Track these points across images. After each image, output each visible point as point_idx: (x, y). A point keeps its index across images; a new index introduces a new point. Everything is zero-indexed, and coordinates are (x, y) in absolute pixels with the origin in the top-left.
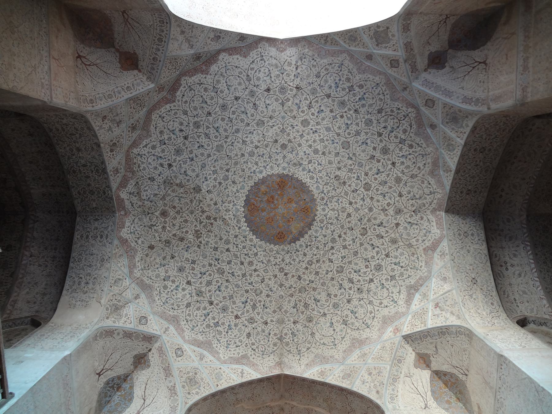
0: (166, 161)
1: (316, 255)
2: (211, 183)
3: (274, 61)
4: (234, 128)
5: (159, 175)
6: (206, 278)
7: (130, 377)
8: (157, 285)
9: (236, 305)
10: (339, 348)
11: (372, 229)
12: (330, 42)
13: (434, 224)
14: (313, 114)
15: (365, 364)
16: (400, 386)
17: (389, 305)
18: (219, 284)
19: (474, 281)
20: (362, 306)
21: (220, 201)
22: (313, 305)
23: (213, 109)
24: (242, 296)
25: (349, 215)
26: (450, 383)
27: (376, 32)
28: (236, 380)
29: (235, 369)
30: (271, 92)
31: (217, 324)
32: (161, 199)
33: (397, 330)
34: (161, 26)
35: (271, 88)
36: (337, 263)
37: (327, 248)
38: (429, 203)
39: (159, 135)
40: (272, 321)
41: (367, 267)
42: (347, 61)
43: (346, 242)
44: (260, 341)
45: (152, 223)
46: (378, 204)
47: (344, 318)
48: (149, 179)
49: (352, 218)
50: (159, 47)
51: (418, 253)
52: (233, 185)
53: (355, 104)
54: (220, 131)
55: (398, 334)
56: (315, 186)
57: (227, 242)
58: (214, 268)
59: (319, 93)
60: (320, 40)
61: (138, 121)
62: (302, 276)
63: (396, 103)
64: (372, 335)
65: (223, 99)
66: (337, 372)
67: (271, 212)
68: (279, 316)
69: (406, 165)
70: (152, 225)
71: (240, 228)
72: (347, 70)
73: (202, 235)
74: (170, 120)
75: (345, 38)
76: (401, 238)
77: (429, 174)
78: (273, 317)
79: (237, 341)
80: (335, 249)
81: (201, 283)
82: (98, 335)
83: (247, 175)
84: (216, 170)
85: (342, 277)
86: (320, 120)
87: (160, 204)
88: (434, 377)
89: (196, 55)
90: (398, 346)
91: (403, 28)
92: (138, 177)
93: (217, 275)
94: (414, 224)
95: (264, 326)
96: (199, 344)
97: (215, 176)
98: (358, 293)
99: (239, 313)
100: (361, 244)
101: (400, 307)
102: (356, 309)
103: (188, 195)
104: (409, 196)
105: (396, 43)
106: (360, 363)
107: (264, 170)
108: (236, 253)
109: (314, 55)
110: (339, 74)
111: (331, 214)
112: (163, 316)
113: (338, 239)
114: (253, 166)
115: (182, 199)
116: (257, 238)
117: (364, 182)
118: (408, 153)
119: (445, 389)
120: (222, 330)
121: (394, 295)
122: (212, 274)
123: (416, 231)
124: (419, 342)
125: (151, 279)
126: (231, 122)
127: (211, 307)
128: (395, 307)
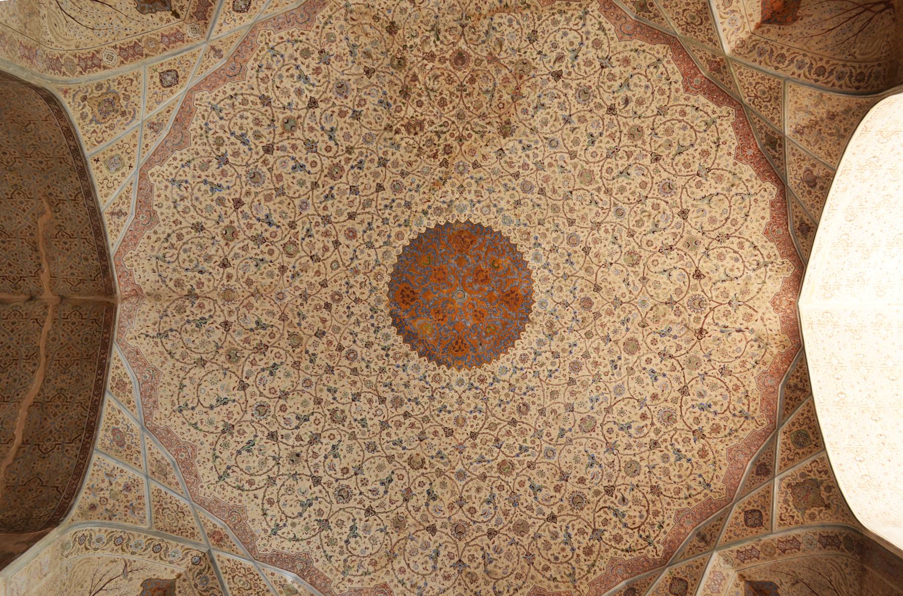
0: (567, 67)
1: (367, 367)
2: (519, 157)
3: (754, 288)
4: (626, 208)
5: (540, 53)
6: (322, 141)
8: (312, 35)
9: (263, 202)
10: (175, 419)
11: (422, 479)
12: (794, 395)
14: (649, 361)
15: (147, 477)
17: (268, 518)
18: (308, 167)
20: (263, 463)
21: (482, 174)
22: (263, 362)
23: (666, 167)
24: (283, 215)
25: (449, 433)
27: (817, 484)
28: (106, 202)
29: (127, 198)
30: (694, 281)
31: (223, 160)
32: (490, 54)
33: (219, 538)
34: (851, 76)
35: (703, 281)
36: (353, 411)
37: (381, 389)
39: (620, 57)
40: (229, 277)
41: (345, 470)
42: (753, 426)
43: (394, 428)
44: (185, 251)
45: (443, 33)
46: (474, 489)
47: (237, 428)
48: (535, 32)
49: (444, 439)
50: (806, 69)
51: (378, 573)
52: (512, 201)
53: (668, 444)
54: (620, 179)
56: (508, 365)
57: (397, 187)
58: (342, 158)
59: (690, 374)
60: (797, 377)
61: (656, 16)
62: (324, 340)
63: (672, 522)
64: (205, 486)
65: (684, 187)
67: (456, 277)
68: (239, 291)
69: (552, 542)
70: (439, 31)
71: (425, 213)
72: (735, 428)
73: (412, 136)
74: (649, 80)
75: (801, 425)
76: (405, 538)
77: (535, 587)
78: (237, 280)
79: (187, 203)
80: (380, 406)
81: (311, 129)
83: (532, 230)
84: (543, 169)
85: (322, 420)
86: (637, 374)
87: (482, 51)
89: (780, 138)
91: (828, 536)
92: (540, 8)
93: (327, 163)
94: (436, 562)
95: (219, 261)
97: (532, 166)
98: (291, 455)
99: (245, 208)
100: (390, 458)
101: (265, 542)
102: (256, 452)
103: (497, 110)
104: (491, 552)
105: (797, 522)
106: (148, 464)
107: (540, 264)
108: (374, 204)
109: (765, 364)
110: (727, 412)
112: (247, 43)
113: (401, 411)
114: (548, 243)
115: (488, 97)
116: (404, 247)
117: (516, 462)
118: (576, 545)
120: (209, 172)
121: (289, 528)
122: (331, 154)
123: (420, 569)
125: (326, 24)
126: (639, 202)
127: (260, 148)
128: (265, 531)
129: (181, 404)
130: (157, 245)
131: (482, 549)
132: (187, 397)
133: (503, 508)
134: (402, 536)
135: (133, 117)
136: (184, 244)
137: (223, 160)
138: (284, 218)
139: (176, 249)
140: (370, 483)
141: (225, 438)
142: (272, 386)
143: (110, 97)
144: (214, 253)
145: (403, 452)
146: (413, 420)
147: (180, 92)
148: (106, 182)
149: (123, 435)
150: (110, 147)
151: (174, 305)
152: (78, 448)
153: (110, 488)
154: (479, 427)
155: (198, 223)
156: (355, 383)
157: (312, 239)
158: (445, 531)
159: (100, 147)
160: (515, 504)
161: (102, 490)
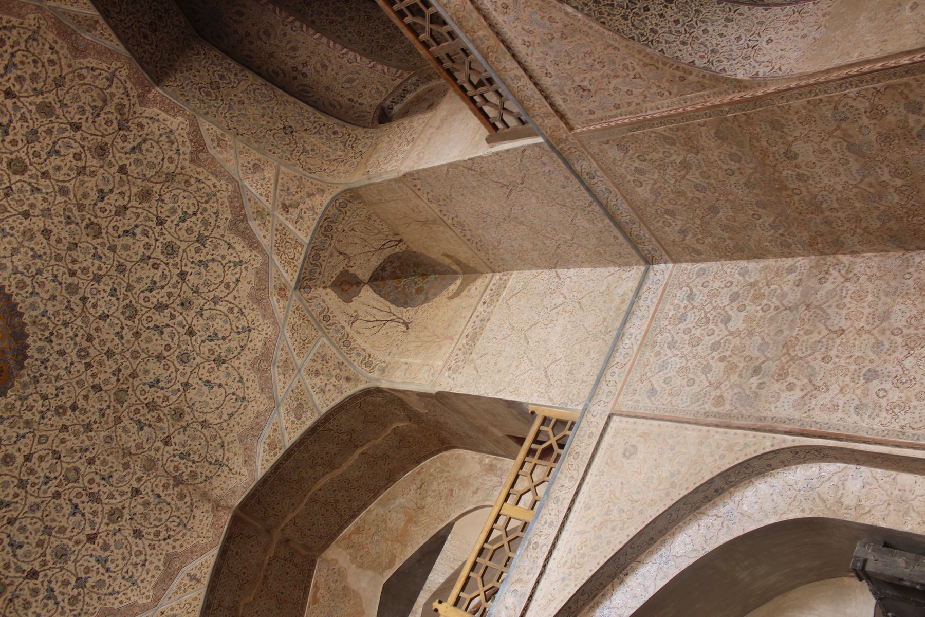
1: (76, 335)
9: (69, 529)
11: (100, 214)
13: (164, 115)
15: (299, 371)
16: (360, 341)
17: (237, 276)
19: (288, 130)
20: (212, 318)
22: (158, 395)
24: (59, 508)
25: (46, 233)
26: (397, 271)
28: (198, 594)
29: (180, 588)
31: (81, 583)
33: (282, 291)
36: (115, 308)
37: (78, 310)
38: (123, 96)
40: (139, 480)
41: (155, 266)
43: (91, 270)
44: (160, 520)
46: (62, 172)
47: (213, 358)
49: (55, 231)
51: (190, 173)
55: (289, 294)
62: (97, 381)
64: (264, 333)
66: (284, 422)
68: (139, 463)
76: (149, 180)
77: (75, 57)
78: (134, 473)
79: (134, 559)
80: (89, 295)
88: (377, 286)
94: (140, 144)
99: (88, 530)
102: (212, 329)
104: (88, 114)
106: (293, 376)
111: (19, 261)
113: (75, 280)
120: (99, 577)
121: (228, 257)
123: (155, 150)
124: (318, 271)
128: (246, 269)
130: (179, 536)
131: (94, 122)
133: (48, 138)
134: (151, 185)
136: (157, 526)
138: (60, 505)
140: (143, 243)
142: (164, 371)
145: (98, 246)
146: (70, 266)
148: (190, 610)
149: (295, 410)
151: (196, 482)
154: (15, 218)
155: (136, 538)
156: (97, 329)
157: (47, 474)
158: (113, 160)
160: (34, 132)
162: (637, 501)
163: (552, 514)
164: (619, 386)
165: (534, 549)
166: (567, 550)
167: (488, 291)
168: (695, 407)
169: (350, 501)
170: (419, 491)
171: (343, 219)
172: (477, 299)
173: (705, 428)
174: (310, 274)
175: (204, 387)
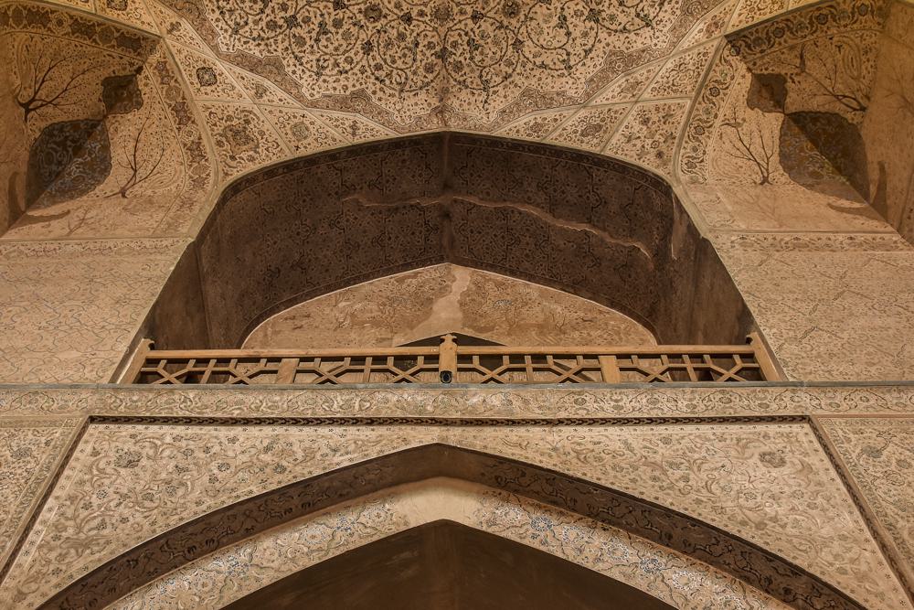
7: (99, 128)
10: (578, 73)
15: (636, 102)
16: (711, 144)
28: (343, 140)
31: (292, 21)
40: (422, 14)
44: (394, 62)
55: (717, 34)
64: (655, 41)
66: (570, 123)
79: (341, 60)
82: (10, 13)
90: (714, 57)
96: (254, 66)
119: (811, 150)
124: (764, 47)
129: (563, 66)
132: (556, 60)
135: (251, 112)
136: (386, 62)
137: (292, 21)
139: (392, 71)
141: (604, 19)
143: (229, 134)
144: (395, 30)
147: (221, 66)
150: (283, 135)
151: (453, 73)
152: (598, 170)
153: (643, 138)
155: (363, 48)
159: (282, 145)
161: (643, 146)
162: (710, 492)
163: (634, 403)
164: (853, 412)
165: (576, 401)
166: (596, 440)
167: (869, 236)
168: (891, 510)
169: (527, 255)
170: (579, 321)
171: (845, 26)
172: (851, 229)
173: (868, 534)
174: (755, 40)
175: (556, 19)
